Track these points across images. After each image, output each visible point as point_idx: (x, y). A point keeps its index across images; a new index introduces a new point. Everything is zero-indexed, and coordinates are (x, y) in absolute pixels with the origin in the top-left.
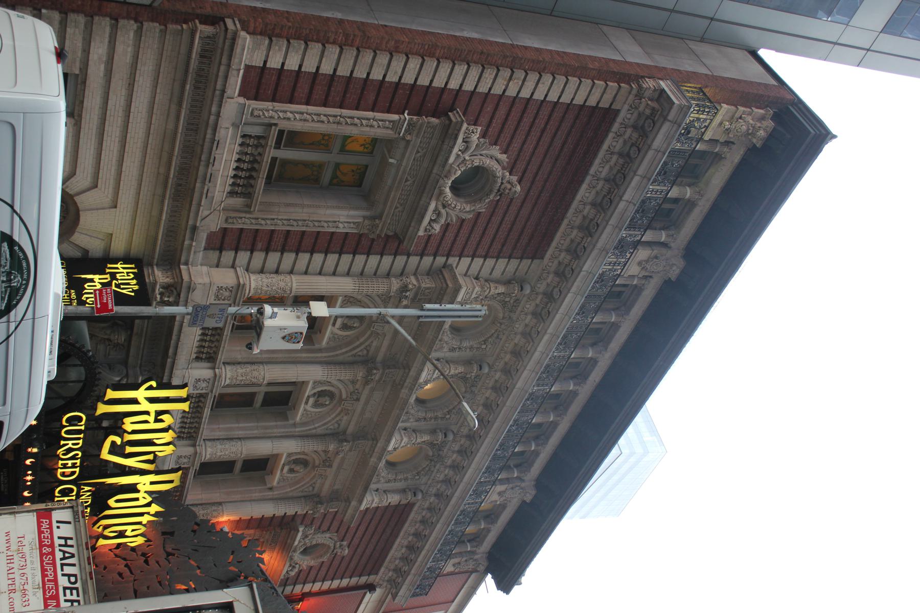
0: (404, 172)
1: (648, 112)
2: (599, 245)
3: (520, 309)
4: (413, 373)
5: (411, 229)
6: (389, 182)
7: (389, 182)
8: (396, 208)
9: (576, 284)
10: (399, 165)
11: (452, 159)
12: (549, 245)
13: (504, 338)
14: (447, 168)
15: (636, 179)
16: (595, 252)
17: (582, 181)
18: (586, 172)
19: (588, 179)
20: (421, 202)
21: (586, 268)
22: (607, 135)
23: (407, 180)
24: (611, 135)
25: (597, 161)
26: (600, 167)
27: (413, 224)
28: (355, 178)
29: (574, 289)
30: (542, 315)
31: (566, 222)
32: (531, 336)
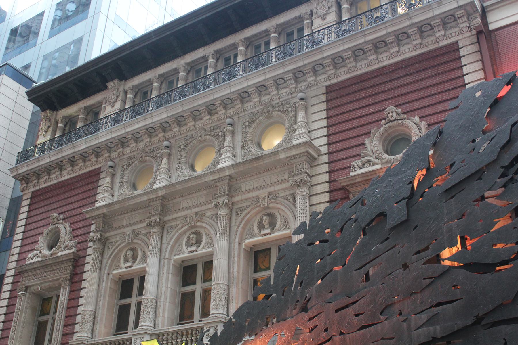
0: (40, 280)
1: (24, 182)
2: (72, 151)
3: (132, 154)
4: (104, 211)
5: (64, 259)
6: (48, 284)
7: (48, 284)
8: (58, 273)
9: (94, 144)
10: (39, 284)
11: (39, 259)
12: (94, 170)
13: (153, 147)
14: (43, 259)
15: (41, 163)
16: (76, 150)
17: (62, 181)
18: (59, 183)
19: (60, 180)
20: (51, 262)
21: (84, 147)
22: (43, 188)
23: (45, 276)
24: (41, 187)
25: (52, 183)
26: (55, 179)
27: (61, 260)
28: (44, 304)
29: (97, 142)
30: (122, 142)
31: (81, 172)
32: (136, 136)
